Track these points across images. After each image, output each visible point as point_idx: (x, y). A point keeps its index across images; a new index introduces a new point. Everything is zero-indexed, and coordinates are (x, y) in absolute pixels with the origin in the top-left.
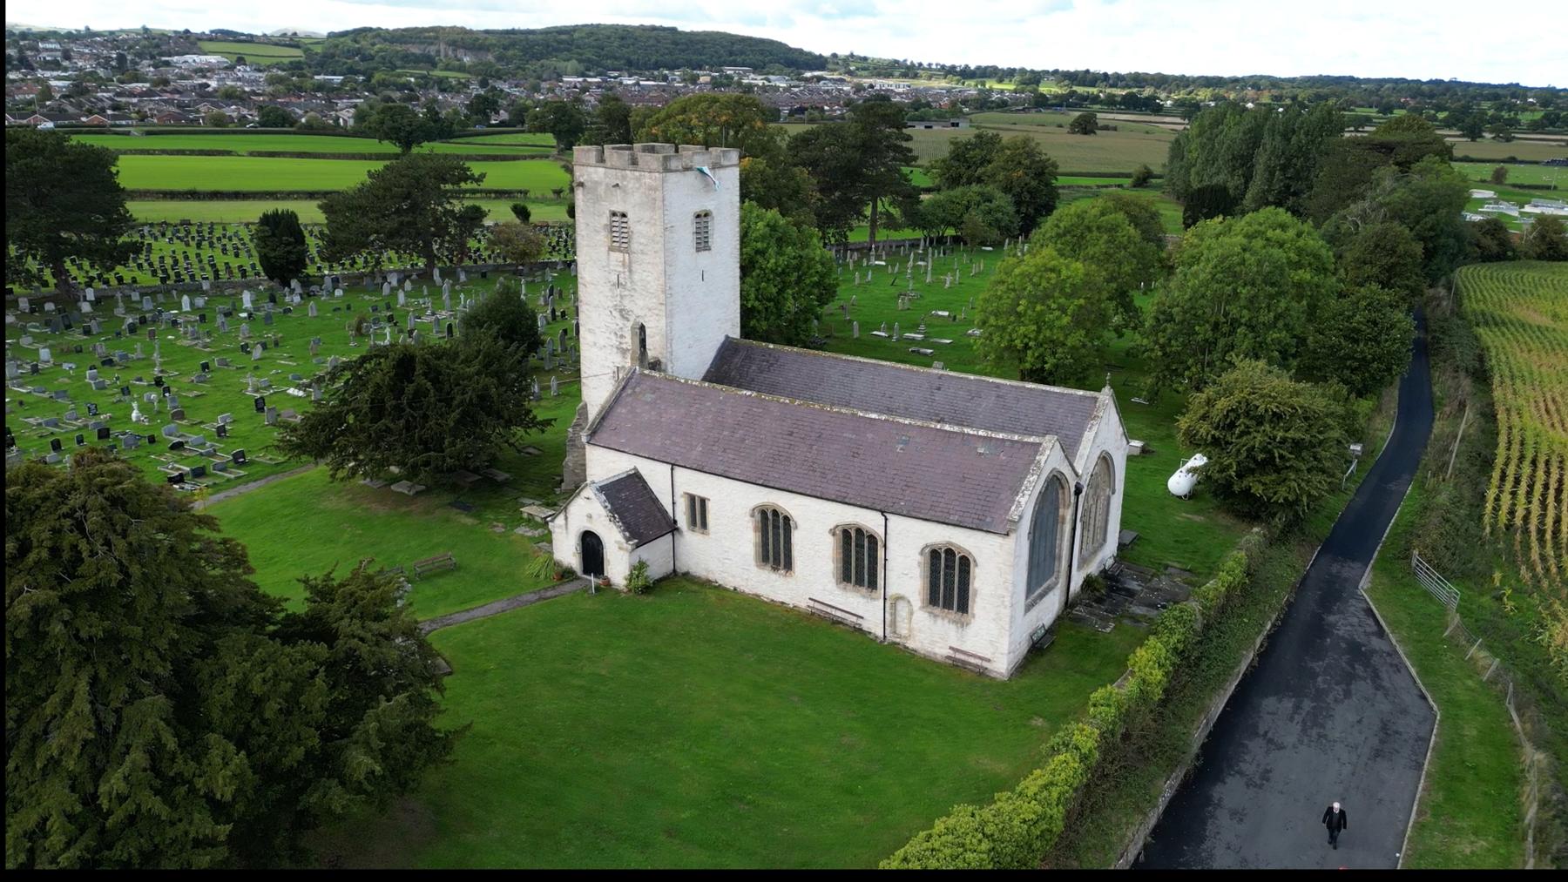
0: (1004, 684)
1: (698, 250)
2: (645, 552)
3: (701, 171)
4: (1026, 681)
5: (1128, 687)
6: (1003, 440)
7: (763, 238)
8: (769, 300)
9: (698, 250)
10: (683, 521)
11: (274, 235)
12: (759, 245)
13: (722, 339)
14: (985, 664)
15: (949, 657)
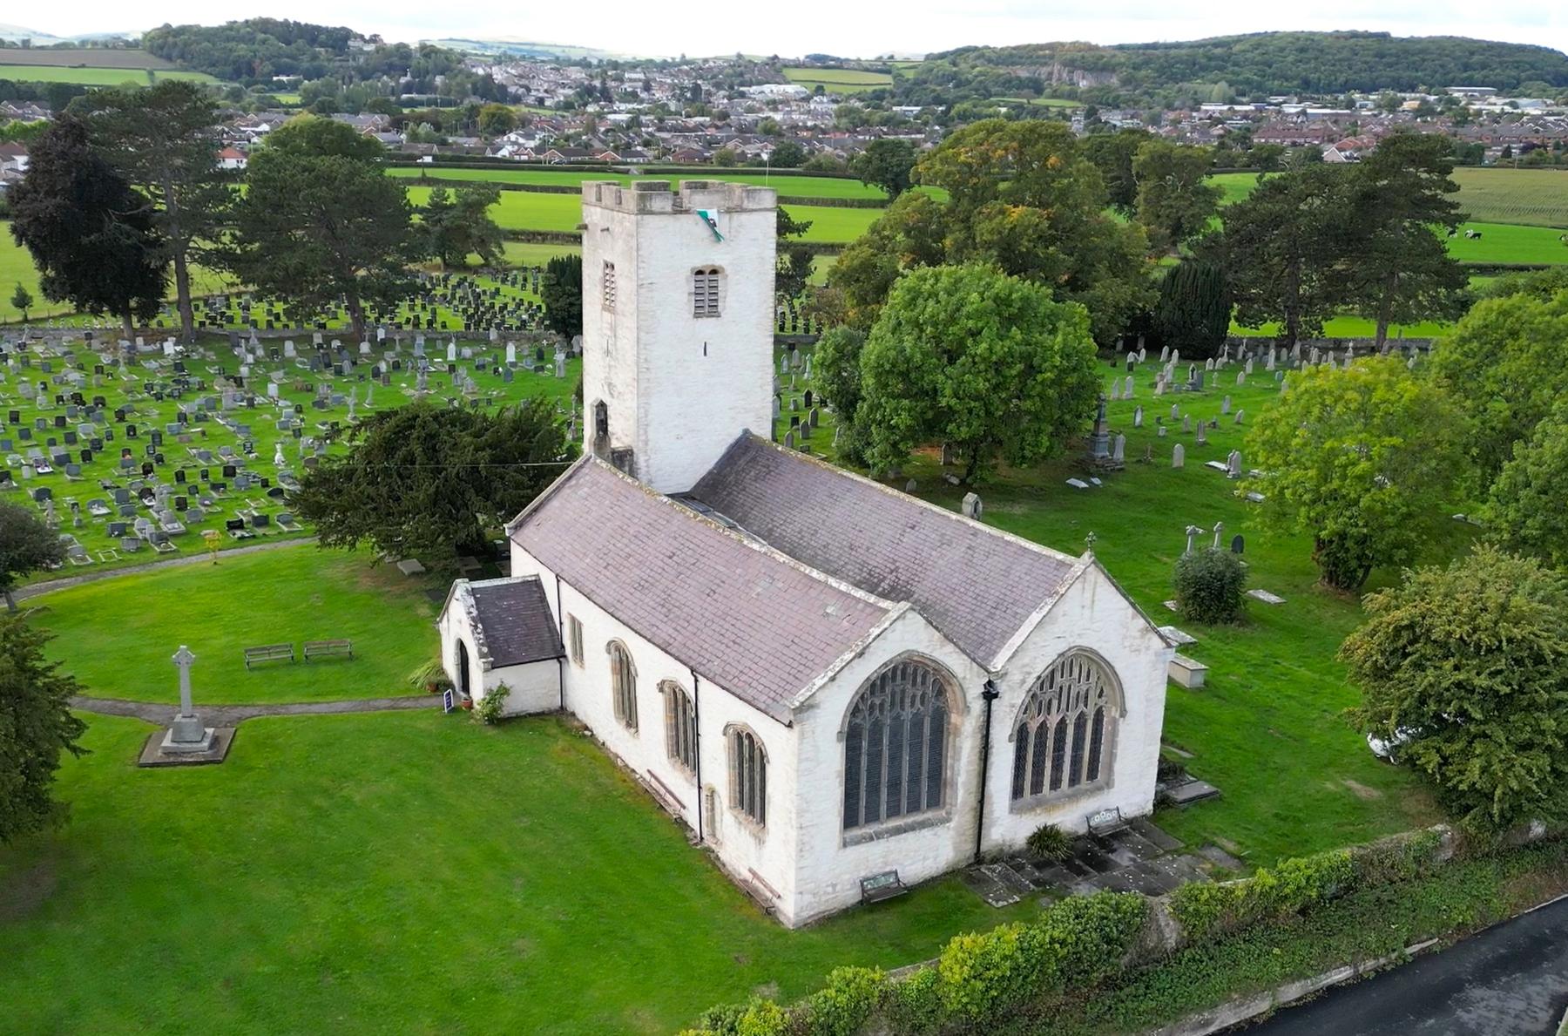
0: (785, 933)
1: (697, 315)
2: (508, 676)
3: (704, 216)
4: (816, 937)
5: (912, 977)
6: (859, 600)
7: (978, 314)
8: (977, 398)
9: (697, 315)
10: (569, 651)
11: (558, 284)
12: (971, 323)
14: (775, 900)
15: (745, 881)
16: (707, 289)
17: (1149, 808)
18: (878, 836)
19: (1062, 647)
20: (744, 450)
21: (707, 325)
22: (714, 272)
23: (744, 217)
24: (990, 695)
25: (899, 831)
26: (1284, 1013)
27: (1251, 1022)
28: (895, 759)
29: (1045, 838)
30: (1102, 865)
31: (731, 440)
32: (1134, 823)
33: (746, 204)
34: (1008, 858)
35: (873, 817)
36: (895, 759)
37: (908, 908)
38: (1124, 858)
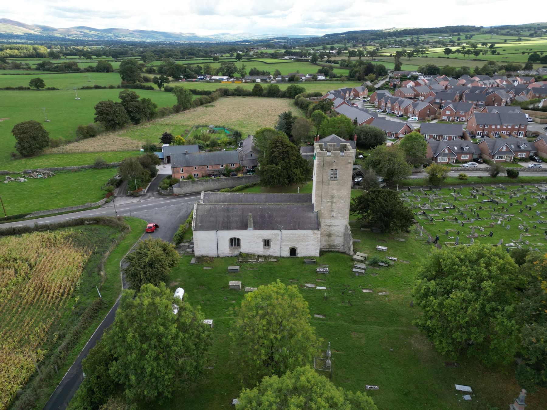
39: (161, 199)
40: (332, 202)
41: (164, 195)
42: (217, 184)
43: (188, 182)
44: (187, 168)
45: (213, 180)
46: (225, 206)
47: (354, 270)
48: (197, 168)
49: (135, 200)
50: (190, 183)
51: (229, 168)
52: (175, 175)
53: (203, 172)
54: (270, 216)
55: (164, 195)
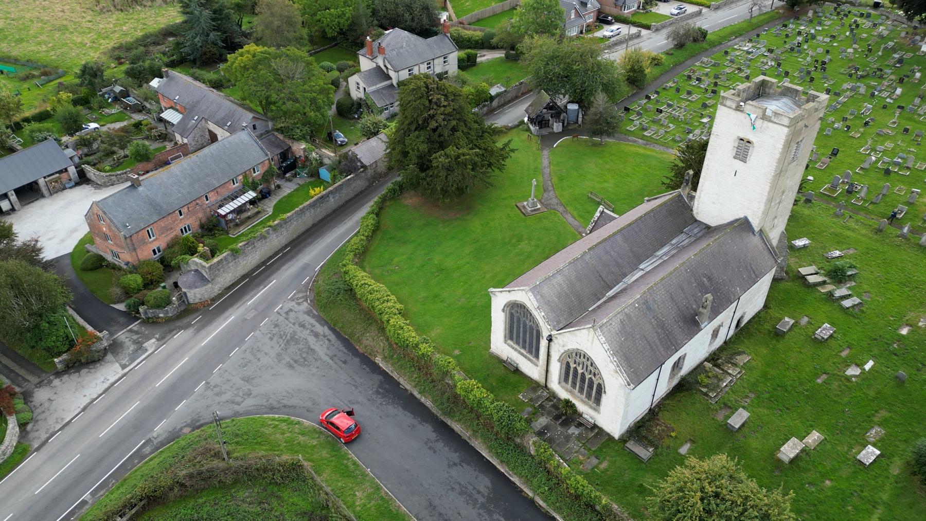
9: (735, 158)
13: (742, 216)
16: (743, 149)
17: (617, 436)
18: (516, 350)
19: (579, 347)
20: (743, 225)
21: (738, 163)
22: (748, 142)
23: (770, 124)
24: (550, 340)
25: (522, 354)
26: (532, 502)
27: (522, 491)
28: (525, 333)
29: (568, 403)
30: (566, 423)
31: (737, 217)
32: (601, 430)
33: (773, 119)
34: (553, 396)
35: (517, 343)
36: (525, 333)
37: (511, 375)
38: (573, 430)
39: (180, 336)
40: (779, 203)
41: (169, 320)
42: (285, 233)
43: (225, 258)
44: (162, 224)
45: (274, 229)
46: (637, 301)
47: (847, 303)
48: (184, 210)
49: (110, 373)
50: (230, 259)
51: (250, 180)
52: (139, 251)
53: (200, 215)
54: (710, 279)
55: (169, 320)
